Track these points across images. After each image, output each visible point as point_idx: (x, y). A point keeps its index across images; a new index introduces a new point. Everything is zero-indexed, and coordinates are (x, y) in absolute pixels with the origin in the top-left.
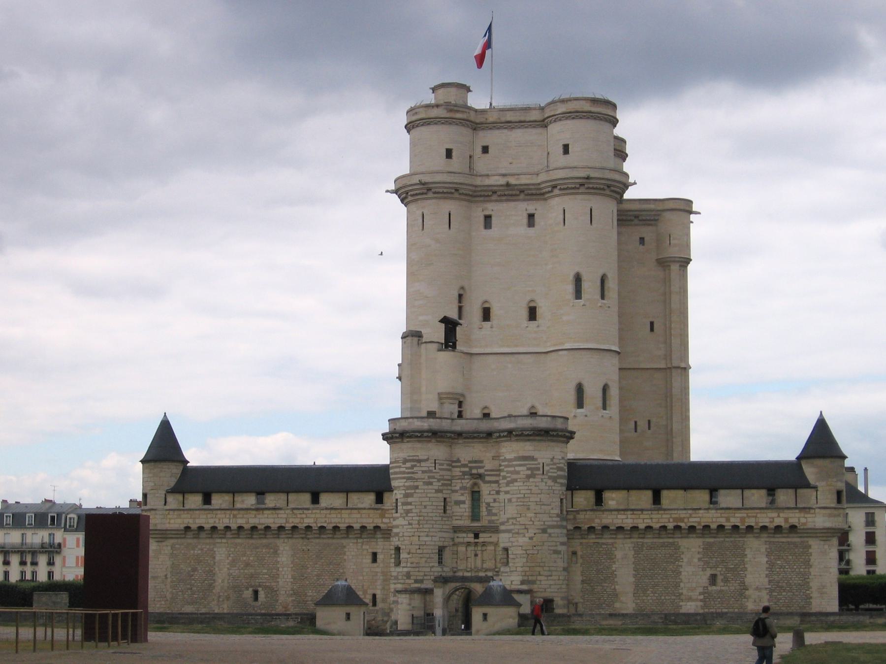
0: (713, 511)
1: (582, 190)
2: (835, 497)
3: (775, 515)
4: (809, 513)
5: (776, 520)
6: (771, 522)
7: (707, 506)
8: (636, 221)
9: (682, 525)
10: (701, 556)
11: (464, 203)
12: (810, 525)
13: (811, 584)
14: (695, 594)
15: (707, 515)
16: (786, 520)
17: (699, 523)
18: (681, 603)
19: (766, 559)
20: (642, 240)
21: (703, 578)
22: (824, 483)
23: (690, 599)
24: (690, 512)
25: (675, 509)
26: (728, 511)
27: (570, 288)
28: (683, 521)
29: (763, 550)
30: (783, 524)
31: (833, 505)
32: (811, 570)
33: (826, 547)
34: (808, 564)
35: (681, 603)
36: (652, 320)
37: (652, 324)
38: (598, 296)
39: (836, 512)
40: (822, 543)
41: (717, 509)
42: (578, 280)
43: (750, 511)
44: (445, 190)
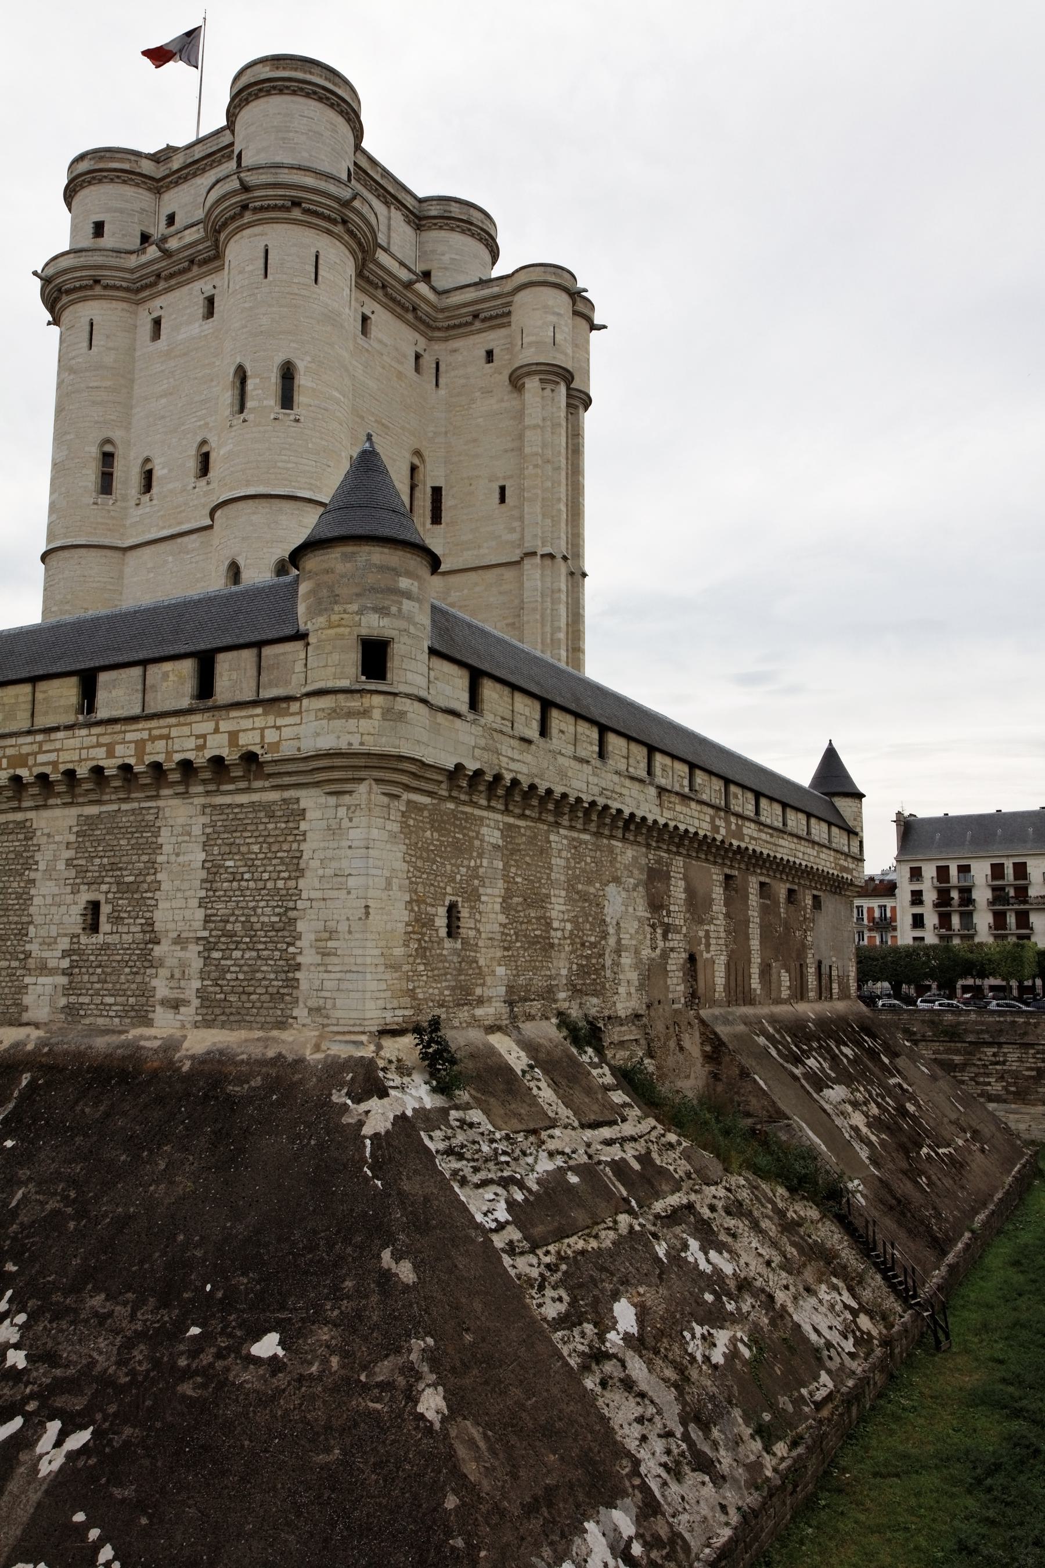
0: (84, 732)
1: (248, 217)
2: (353, 658)
3: (210, 726)
4: (287, 713)
5: (211, 741)
6: (201, 748)
7: (70, 718)
8: (478, 325)
9: (23, 772)
10: (70, 854)
11: (125, 305)
12: (288, 750)
13: (300, 926)
14: (54, 958)
15: (71, 743)
16: (233, 736)
17: (55, 764)
18: (27, 980)
19: (202, 856)
20: (490, 355)
21: (73, 917)
22: (321, 620)
23: (43, 969)
24: (39, 738)
25: (11, 735)
26: (110, 729)
27: (227, 397)
28: (24, 765)
29: (197, 830)
30: (224, 753)
31: (345, 683)
32: (302, 883)
33: (342, 812)
34: (296, 867)
35: (27, 980)
36: (502, 483)
37: (503, 489)
38: (272, 402)
39: (354, 703)
40: (332, 800)
41: (89, 725)
42: (241, 376)
43: (153, 723)
44: (77, 284)
